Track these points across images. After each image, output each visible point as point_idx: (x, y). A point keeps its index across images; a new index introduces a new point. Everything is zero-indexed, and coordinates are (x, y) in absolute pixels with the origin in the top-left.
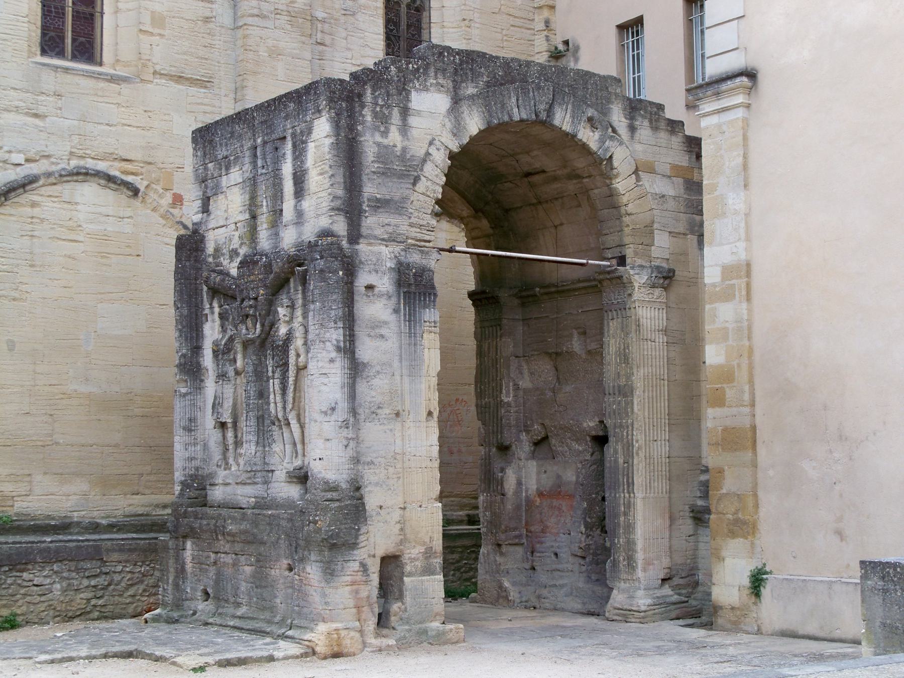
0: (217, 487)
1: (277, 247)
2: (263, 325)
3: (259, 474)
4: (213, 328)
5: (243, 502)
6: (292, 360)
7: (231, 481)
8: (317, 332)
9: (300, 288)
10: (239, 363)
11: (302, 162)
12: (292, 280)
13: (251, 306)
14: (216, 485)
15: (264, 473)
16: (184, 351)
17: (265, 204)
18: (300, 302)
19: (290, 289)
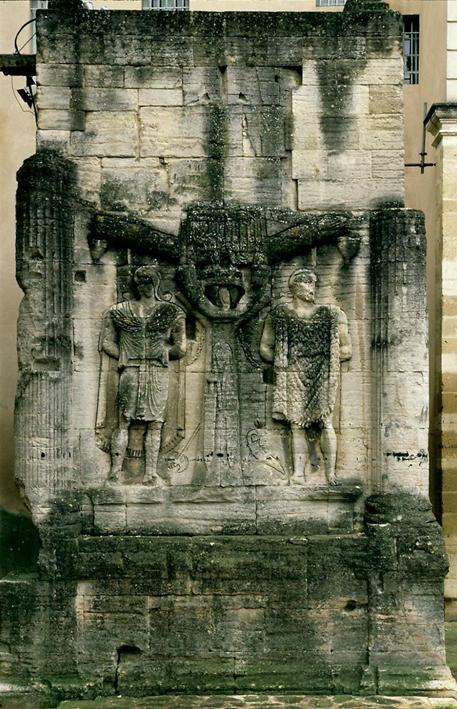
0: (123, 508)
1: (275, 205)
2: (254, 300)
4: (96, 292)
5: (197, 526)
6: (335, 350)
8: (413, 321)
9: (337, 261)
11: (341, 106)
12: (314, 252)
13: (238, 275)
14: (120, 504)
15: (245, 490)
16: (54, 320)
17: (246, 142)
18: (334, 278)
19: (311, 261)
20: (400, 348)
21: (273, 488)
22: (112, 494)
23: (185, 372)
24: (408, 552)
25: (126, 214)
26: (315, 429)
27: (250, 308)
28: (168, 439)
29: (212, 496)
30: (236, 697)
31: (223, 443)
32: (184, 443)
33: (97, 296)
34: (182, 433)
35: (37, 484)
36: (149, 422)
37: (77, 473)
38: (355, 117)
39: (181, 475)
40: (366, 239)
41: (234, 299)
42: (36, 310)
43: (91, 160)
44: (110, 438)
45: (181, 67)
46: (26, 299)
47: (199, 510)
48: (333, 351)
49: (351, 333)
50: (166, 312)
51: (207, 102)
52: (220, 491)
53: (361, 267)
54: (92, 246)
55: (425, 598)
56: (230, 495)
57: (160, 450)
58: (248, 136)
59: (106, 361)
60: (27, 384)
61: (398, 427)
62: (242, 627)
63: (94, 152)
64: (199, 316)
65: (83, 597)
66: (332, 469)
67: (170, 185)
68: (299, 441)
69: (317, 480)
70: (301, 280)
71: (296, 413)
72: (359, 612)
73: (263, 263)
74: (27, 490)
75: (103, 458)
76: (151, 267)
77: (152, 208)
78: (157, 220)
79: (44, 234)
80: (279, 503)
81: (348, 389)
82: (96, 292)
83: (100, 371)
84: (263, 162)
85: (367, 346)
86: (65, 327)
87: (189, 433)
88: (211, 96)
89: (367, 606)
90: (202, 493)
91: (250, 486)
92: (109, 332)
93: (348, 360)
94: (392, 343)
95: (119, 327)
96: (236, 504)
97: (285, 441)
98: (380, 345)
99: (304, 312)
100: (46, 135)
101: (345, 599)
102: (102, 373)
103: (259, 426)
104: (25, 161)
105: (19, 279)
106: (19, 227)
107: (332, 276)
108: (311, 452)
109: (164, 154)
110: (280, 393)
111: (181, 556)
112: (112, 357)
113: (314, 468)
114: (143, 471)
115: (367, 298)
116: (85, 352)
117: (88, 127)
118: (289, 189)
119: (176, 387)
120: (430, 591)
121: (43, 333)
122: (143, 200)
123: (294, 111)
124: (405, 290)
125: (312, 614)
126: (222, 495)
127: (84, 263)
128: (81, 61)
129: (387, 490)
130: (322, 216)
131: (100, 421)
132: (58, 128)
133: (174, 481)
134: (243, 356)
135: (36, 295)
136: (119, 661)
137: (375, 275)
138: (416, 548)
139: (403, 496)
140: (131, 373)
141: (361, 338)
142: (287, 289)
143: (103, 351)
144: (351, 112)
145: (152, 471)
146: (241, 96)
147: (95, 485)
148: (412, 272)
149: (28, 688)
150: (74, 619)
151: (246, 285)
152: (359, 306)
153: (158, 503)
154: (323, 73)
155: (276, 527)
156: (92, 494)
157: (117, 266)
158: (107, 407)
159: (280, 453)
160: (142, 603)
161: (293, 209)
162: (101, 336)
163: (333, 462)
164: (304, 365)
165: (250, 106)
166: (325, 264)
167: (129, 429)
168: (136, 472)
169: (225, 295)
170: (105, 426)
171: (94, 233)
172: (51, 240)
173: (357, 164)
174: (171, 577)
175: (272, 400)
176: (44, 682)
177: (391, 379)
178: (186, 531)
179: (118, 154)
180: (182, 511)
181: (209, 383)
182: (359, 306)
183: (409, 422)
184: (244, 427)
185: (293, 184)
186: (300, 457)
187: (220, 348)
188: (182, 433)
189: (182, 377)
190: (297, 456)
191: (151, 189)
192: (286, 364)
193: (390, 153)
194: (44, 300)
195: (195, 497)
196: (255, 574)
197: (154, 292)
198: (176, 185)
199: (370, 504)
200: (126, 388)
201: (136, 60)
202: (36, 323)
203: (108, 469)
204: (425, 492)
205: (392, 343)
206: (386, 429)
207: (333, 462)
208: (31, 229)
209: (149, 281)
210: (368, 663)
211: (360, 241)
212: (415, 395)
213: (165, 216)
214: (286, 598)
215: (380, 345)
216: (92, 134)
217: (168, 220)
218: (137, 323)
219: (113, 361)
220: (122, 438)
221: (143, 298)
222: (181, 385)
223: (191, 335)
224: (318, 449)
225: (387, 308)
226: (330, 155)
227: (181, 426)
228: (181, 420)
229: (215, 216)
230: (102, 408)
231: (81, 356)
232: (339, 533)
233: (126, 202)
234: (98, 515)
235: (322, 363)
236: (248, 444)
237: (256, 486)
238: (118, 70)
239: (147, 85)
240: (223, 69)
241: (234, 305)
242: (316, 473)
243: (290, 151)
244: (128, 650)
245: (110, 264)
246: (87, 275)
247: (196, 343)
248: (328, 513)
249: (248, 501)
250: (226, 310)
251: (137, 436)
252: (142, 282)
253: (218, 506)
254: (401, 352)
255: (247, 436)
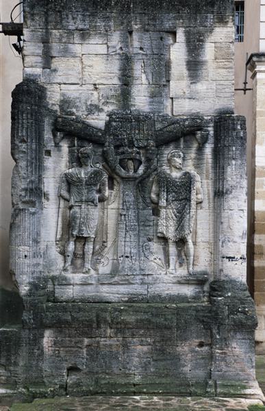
0: (72, 286)
1: (160, 112)
2: (147, 168)
3: (138, 277)
4: (57, 163)
6: (193, 197)
7: (93, 282)
8: (238, 180)
9: (195, 145)
10: (107, 193)
11: (198, 55)
12: (182, 140)
13: (138, 153)
14: (71, 284)
15: (141, 277)
16: (33, 178)
18: (193, 155)
19: (180, 145)
20: (230, 196)
21: (158, 276)
22: (65, 279)
23: (107, 209)
24: (234, 314)
25: (74, 117)
26: (181, 242)
27: (145, 172)
28: (97, 247)
29: (122, 280)
30: (135, 397)
31: (129, 250)
32: (106, 249)
33: (57, 165)
34: (105, 244)
35: (23, 273)
36: (86, 238)
37: (45, 266)
38: (206, 62)
39: (105, 268)
40: (212, 133)
41: (136, 168)
42: (22, 172)
43: (55, 86)
44: (64, 247)
45: (107, 31)
46: (16, 166)
47: (115, 289)
48: (192, 197)
49: (202, 187)
50: (97, 174)
51: (121, 52)
52: (127, 278)
53: (208, 149)
54: (55, 136)
55: (243, 341)
56: (133, 280)
57: (93, 253)
58: (145, 72)
59: (62, 202)
60: (17, 215)
61: (229, 241)
62: (139, 356)
63: (56, 81)
64: (116, 176)
65: (48, 338)
66: (191, 265)
67: (99, 100)
68: (172, 249)
69: (182, 272)
70: (174, 156)
71: (171, 233)
72: (205, 348)
73: (153, 146)
74: (16, 277)
75: (60, 259)
76: (89, 148)
77: (89, 114)
78: (92, 121)
79: (27, 128)
80: (161, 285)
81: (201, 220)
82: (57, 163)
83: (59, 208)
84: (153, 88)
85: (212, 195)
86: (39, 183)
87: (109, 244)
88: (124, 49)
89: (210, 345)
90: (116, 279)
91: (143, 275)
92: (64, 186)
93: (201, 203)
94: (226, 193)
95: (70, 182)
96: (136, 285)
97: (164, 249)
98: (220, 194)
99: (176, 174)
100: (28, 70)
101: (198, 341)
102: (60, 210)
103: (150, 240)
104: (17, 86)
105: (13, 154)
106: (13, 124)
107: (192, 154)
108: (179, 256)
109: (97, 83)
110: (162, 222)
111: (104, 315)
112: (66, 200)
113: (181, 265)
114: (83, 266)
115: (212, 167)
116: (50, 197)
117: (53, 66)
118: (168, 103)
119: (102, 218)
120: (247, 337)
121: (26, 186)
122: (84, 109)
123: (171, 57)
124: (234, 162)
125: (179, 349)
126: (128, 280)
127: (50, 145)
128: (49, 27)
129: (223, 278)
130: (187, 119)
131: (59, 237)
132: (36, 66)
133: (100, 272)
134: (141, 200)
135: (23, 164)
136: (68, 376)
137: (217, 153)
138: (239, 312)
139: (232, 282)
140: (76, 209)
141: (208, 190)
142: (166, 161)
143: (60, 196)
144: (204, 59)
145: (88, 266)
146: (141, 49)
147: (56, 273)
148: (238, 152)
149: (15, 391)
150: (42, 351)
151: (143, 159)
152: (207, 171)
153: (91, 284)
154: (188, 35)
155: (158, 298)
156: (54, 278)
157: (69, 147)
158: (63, 229)
159: (162, 256)
160: (82, 342)
161: (170, 115)
162: (60, 188)
163: (191, 262)
164: (175, 205)
165: (146, 55)
166: (188, 147)
167: (75, 241)
168: (79, 266)
169: (131, 164)
170: (61, 239)
171: (55, 130)
172: (31, 132)
173: (207, 89)
174: (98, 327)
175: (157, 225)
176: (25, 388)
177: (225, 214)
178: (107, 300)
179: (70, 82)
180: (105, 289)
181: (121, 215)
182: (207, 171)
183: (236, 239)
184: (141, 241)
185: (170, 100)
186: (173, 259)
187: (127, 195)
188: (105, 244)
189: (106, 212)
190: (171, 258)
191: (89, 103)
192: (165, 205)
193: (227, 83)
194: (27, 166)
195: (113, 280)
196: (146, 326)
197: (90, 162)
198: (103, 101)
199: (212, 285)
200: (73, 218)
201: (80, 27)
202: (22, 180)
203: (63, 265)
204: (244, 280)
205: (226, 193)
206: (222, 243)
207: (191, 262)
208: (20, 126)
209: (87, 157)
210: (211, 378)
211: (208, 134)
212: (238, 223)
213: (96, 119)
214: (164, 340)
215: (220, 194)
216: (55, 70)
217: (99, 121)
218: (80, 180)
219: (66, 202)
220: (71, 247)
221: (84, 166)
222: (105, 217)
223: (111, 188)
224: (183, 254)
225: (223, 172)
226: (191, 83)
227: (104, 240)
228: (105, 236)
229: (125, 119)
230: (59, 229)
231: (48, 199)
232: (195, 302)
233: (74, 110)
234: (57, 290)
235: (186, 204)
236: (143, 250)
237: (148, 275)
238: (70, 33)
239: (87, 42)
240: (131, 33)
241: (136, 171)
242: (182, 268)
243: (168, 81)
244: (73, 369)
245: (65, 147)
246: (52, 152)
247: (114, 192)
248: (188, 291)
249: (143, 283)
250: (131, 173)
251: (79, 246)
252: (83, 157)
253: (126, 286)
254: (232, 198)
255: (143, 246)
